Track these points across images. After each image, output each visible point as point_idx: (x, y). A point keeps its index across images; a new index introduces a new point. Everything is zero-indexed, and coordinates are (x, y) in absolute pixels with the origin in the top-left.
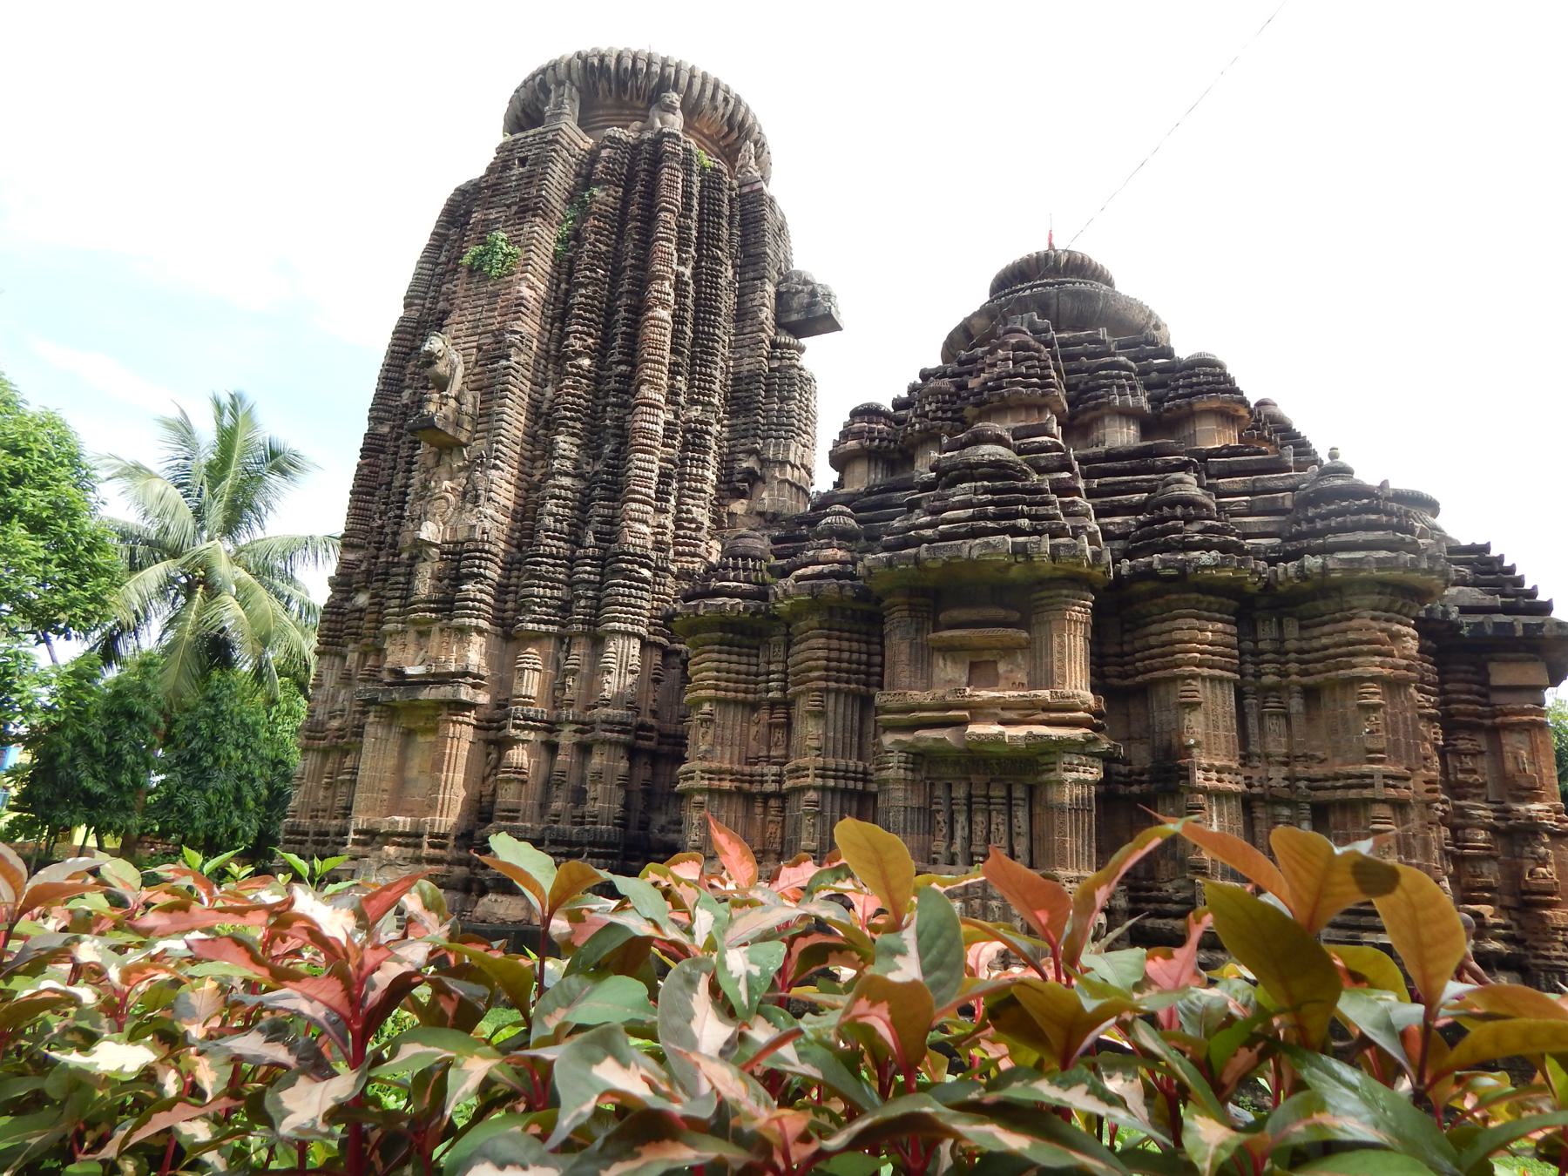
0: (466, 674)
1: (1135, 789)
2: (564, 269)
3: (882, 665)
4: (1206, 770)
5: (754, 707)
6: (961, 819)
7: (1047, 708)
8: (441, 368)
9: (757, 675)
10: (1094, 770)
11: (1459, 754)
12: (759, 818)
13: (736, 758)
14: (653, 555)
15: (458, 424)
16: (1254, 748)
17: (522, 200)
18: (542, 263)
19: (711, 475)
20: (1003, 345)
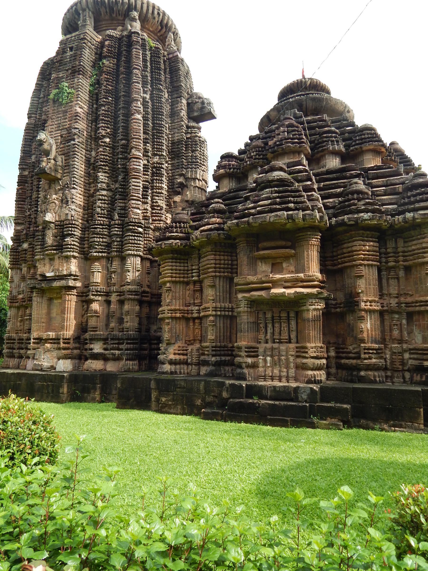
0: (71, 275)
1: (338, 310)
2: (94, 98)
3: (237, 265)
4: (365, 302)
5: (187, 283)
6: (270, 326)
7: (302, 281)
8: (46, 146)
9: (188, 270)
10: (321, 304)
12: (191, 327)
13: (181, 304)
14: (143, 222)
15: (56, 171)
16: (385, 292)
17: (73, 67)
18: (84, 96)
19: (165, 186)
20: (283, 125)
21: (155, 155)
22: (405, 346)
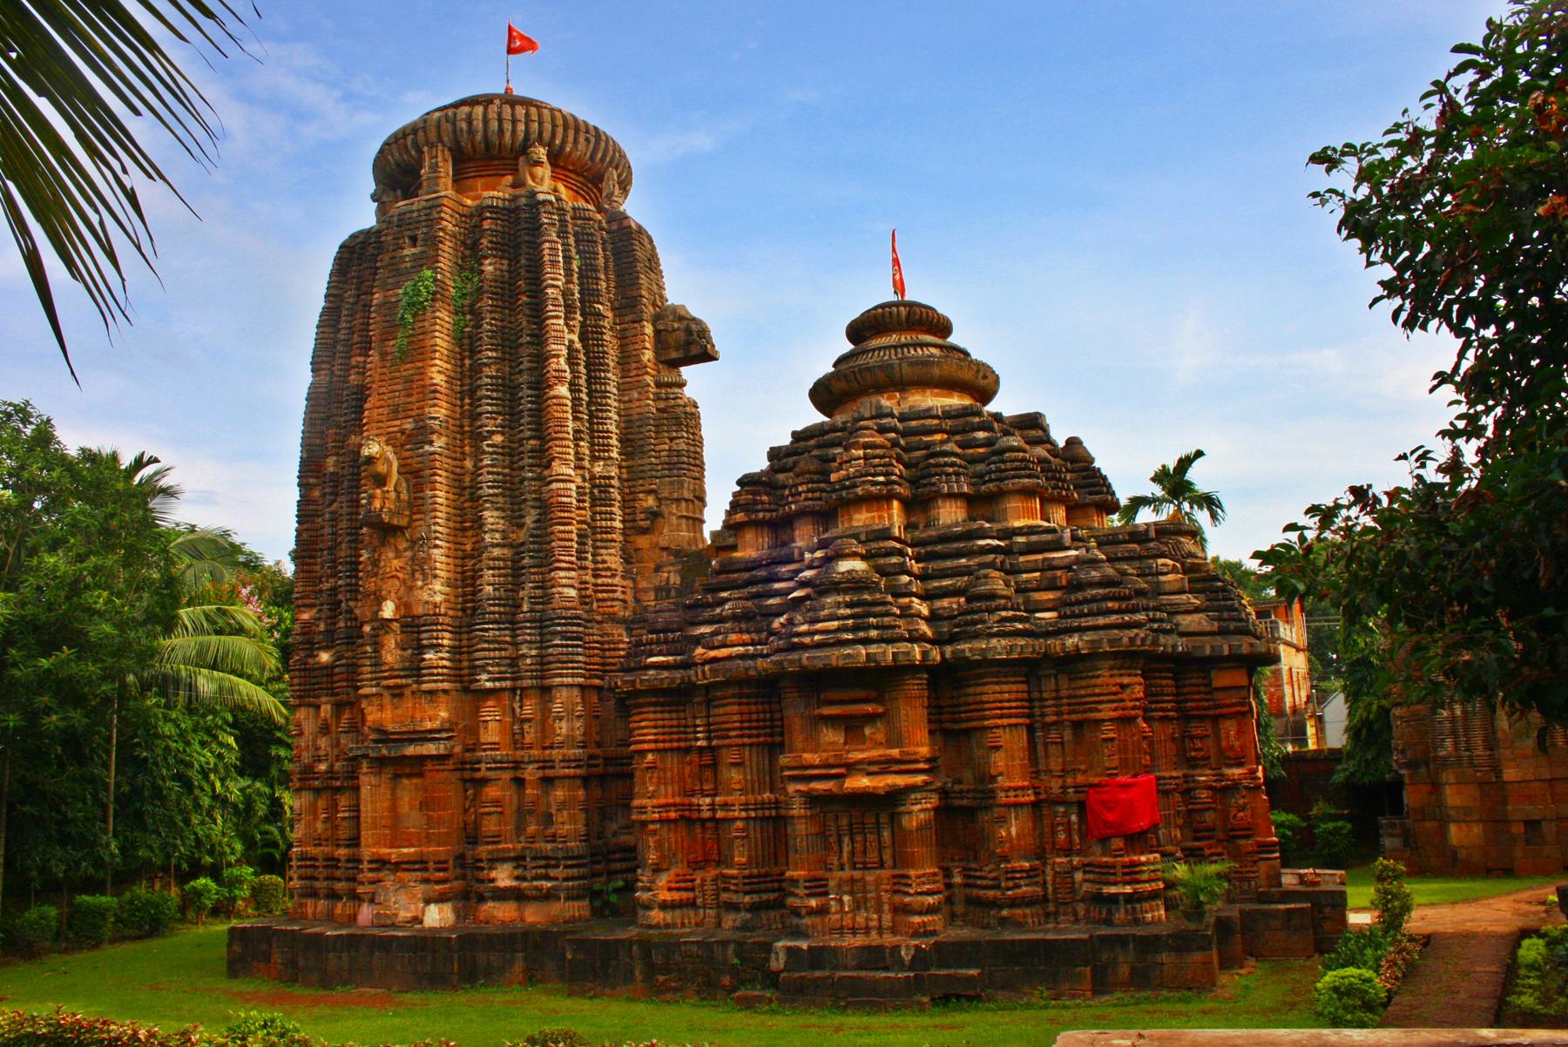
1: (965, 802)
2: (466, 345)
3: (782, 719)
5: (688, 750)
6: (846, 839)
8: (381, 468)
11: (1192, 738)
21: (594, 459)
22: (1076, 860)
